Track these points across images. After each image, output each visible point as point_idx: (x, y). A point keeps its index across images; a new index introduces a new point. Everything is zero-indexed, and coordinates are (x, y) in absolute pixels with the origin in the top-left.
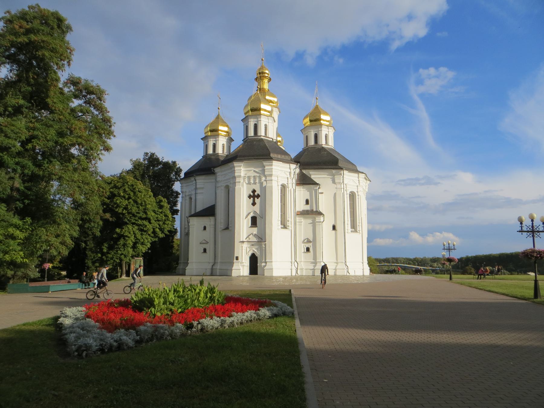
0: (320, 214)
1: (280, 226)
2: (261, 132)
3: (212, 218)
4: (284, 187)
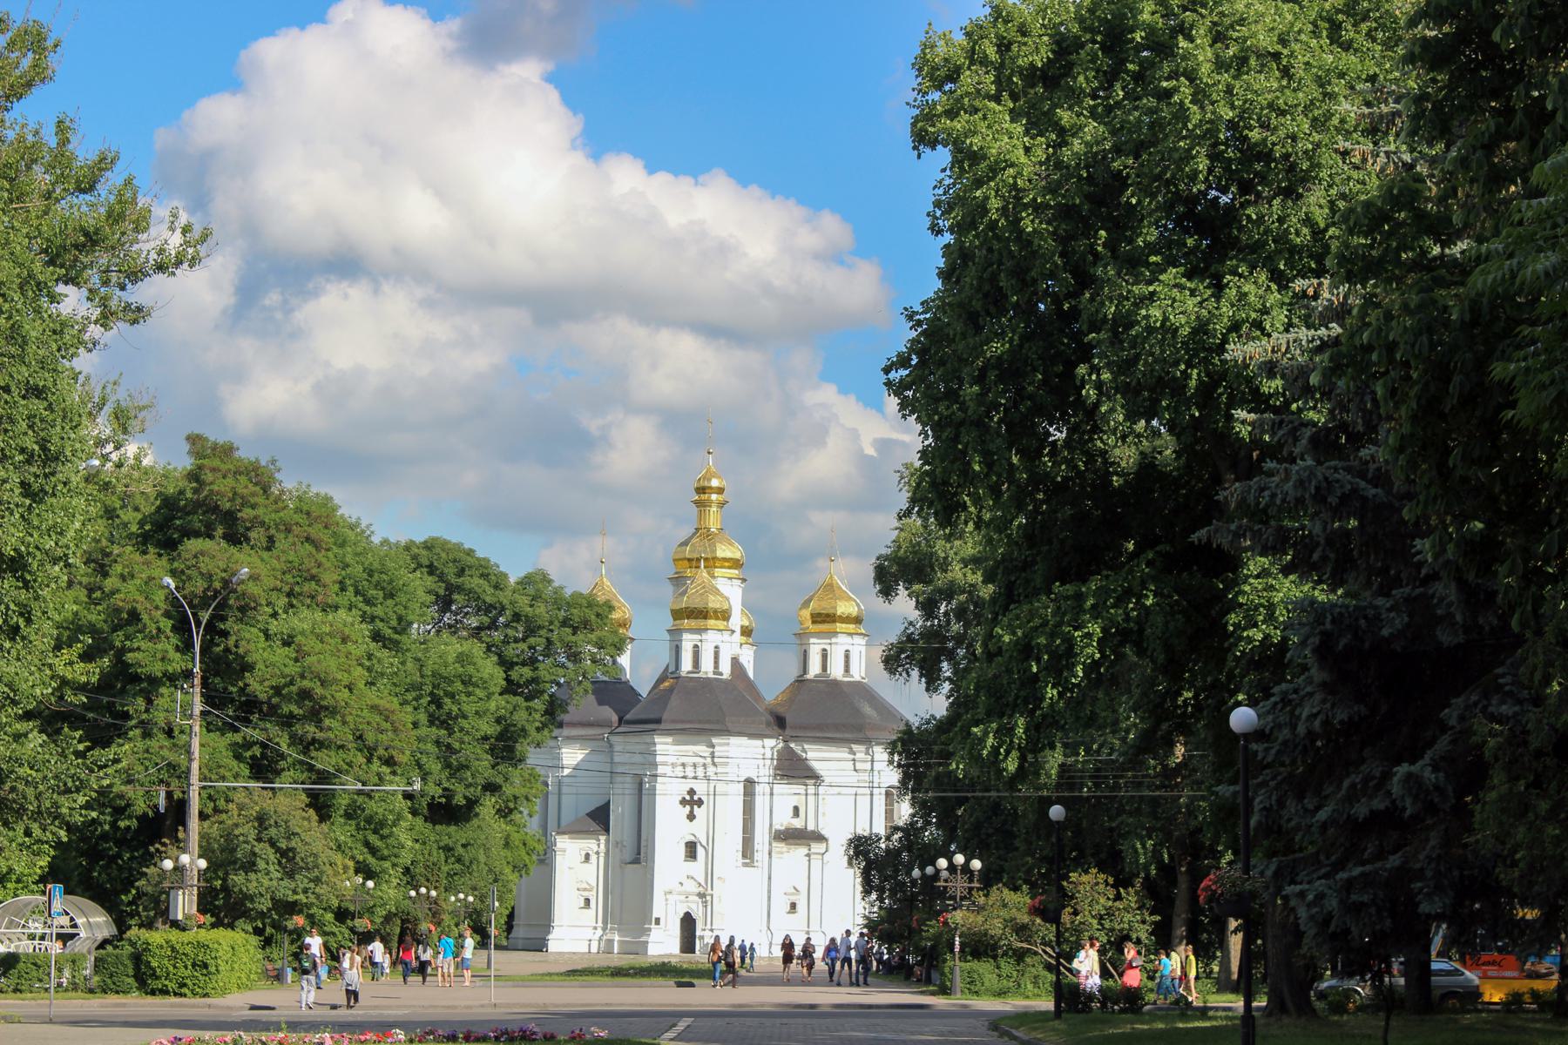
0: (819, 838)
1: (741, 861)
2: (707, 666)
3: (603, 838)
4: (749, 784)
